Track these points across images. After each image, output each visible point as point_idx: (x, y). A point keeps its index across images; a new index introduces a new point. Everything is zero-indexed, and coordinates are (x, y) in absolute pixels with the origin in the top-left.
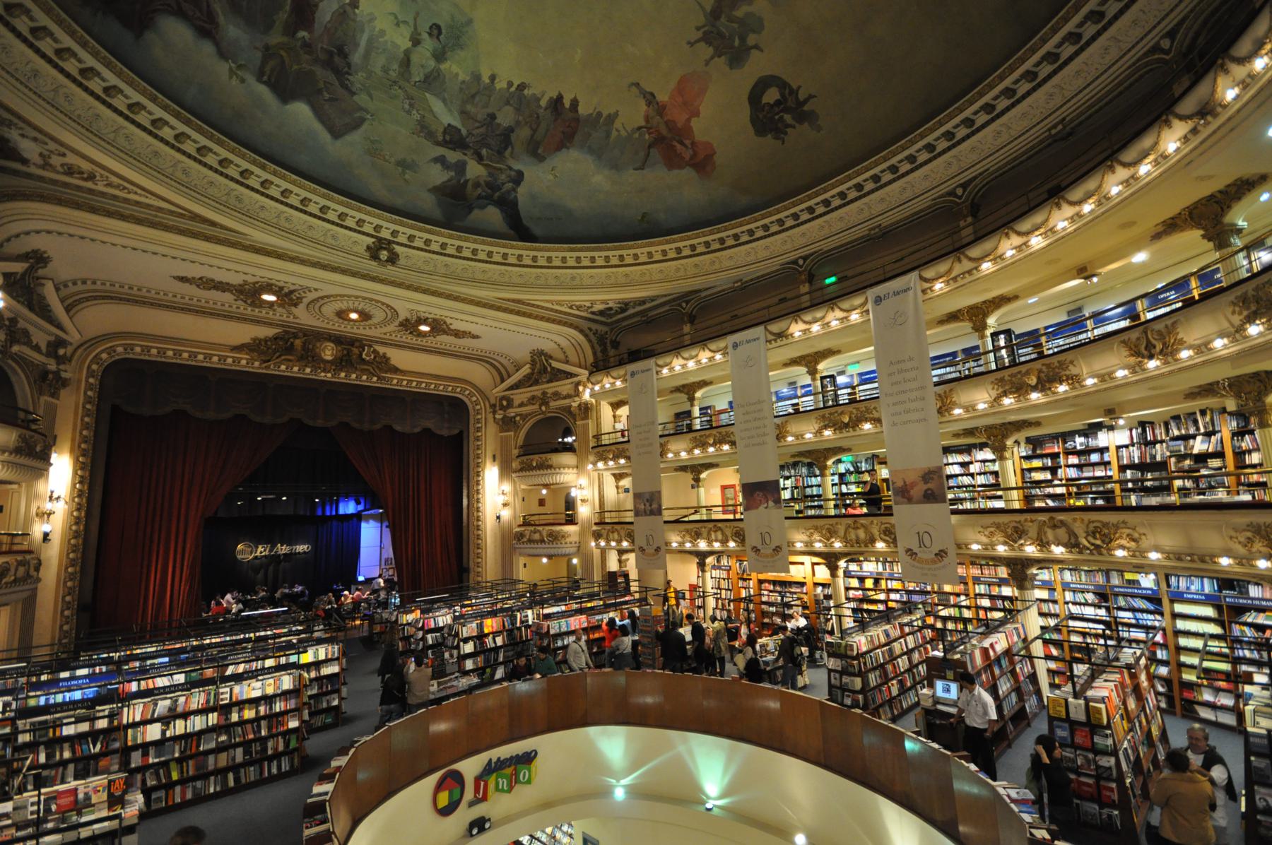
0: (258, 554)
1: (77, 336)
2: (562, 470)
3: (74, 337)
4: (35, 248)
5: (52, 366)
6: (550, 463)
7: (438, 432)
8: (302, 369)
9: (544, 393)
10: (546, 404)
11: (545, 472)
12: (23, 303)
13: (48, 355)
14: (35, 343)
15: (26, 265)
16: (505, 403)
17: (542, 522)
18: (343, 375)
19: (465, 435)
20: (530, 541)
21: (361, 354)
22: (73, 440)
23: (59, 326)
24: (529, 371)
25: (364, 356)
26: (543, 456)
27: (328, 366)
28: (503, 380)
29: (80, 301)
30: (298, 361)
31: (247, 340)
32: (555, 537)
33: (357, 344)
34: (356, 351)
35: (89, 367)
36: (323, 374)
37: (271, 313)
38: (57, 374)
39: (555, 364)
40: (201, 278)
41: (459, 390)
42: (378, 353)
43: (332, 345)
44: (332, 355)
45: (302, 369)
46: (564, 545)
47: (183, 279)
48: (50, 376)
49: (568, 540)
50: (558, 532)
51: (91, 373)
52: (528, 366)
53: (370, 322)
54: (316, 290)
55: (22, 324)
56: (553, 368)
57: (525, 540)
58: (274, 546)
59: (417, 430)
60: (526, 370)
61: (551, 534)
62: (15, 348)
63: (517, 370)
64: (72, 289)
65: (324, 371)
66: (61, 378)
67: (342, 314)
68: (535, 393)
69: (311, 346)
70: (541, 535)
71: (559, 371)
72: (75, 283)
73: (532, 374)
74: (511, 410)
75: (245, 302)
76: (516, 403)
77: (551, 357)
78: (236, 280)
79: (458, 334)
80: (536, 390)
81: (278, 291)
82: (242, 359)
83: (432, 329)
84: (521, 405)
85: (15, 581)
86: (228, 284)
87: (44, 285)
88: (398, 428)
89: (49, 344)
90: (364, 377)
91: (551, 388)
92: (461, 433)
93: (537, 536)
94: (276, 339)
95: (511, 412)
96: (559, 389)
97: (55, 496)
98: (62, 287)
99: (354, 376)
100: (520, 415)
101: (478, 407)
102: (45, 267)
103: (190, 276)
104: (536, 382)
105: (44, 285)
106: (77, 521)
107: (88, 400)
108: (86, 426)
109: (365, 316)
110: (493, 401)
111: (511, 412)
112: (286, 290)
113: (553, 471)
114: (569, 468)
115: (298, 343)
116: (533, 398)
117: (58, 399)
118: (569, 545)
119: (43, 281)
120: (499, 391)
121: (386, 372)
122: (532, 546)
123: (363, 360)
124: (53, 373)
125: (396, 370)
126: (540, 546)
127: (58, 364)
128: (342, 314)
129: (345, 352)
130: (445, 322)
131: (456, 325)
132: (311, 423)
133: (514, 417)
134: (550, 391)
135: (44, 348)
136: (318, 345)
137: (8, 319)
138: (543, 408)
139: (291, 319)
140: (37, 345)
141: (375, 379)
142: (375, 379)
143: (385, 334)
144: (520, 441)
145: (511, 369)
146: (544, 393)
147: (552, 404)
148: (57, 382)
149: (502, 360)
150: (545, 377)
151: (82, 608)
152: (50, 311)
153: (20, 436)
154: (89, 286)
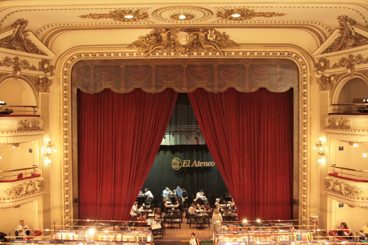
0: (184, 166)
1: (53, 55)
2: (357, 132)
3: (51, 56)
4: (18, 19)
5: (41, 75)
6: (348, 124)
7: (272, 90)
8: (169, 53)
9: (351, 56)
10: (351, 66)
11: (344, 132)
12: (19, 49)
13: (40, 70)
14: (31, 66)
15: (17, 29)
16: (322, 64)
17: (344, 176)
18: (195, 54)
19: (295, 91)
20: (333, 190)
21: (206, 36)
22: (60, 112)
23: (43, 53)
24: (339, 35)
25: (209, 38)
26: (344, 116)
27: (183, 49)
28: (322, 42)
29: (52, 35)
30: (165, 48)
31: (135, 39)
32: (350, 191)
33: (201, 30)
34: (202, 35)
35: (63, 70)
36: (182, 56)
37: (138, 23)
38: (46, 80)
39: (357, 30)
40: (90, 15)
41: (286, 54)
42: (219, 33)
43: (186, 33)
44: (187, 40)
45: (169, 53)
46: (356, 200)
47: (84, 17)
48: (41, 81)
49: (360, 195)
50: (352, 188)
51: (65, 73)
52: (337, 31)
53: (195, 18)
54: (148, 8)
55: (21, 59)
56: (356, 33)
57: (330, 188)
58: (192, 161)
59: (254, 90)
60: (336, 34)
61: (347, 189)
62: (18, 73)
63: (331, 34)
64: (45, 31)
65: (182, 53)
66: (48, 80)
67: (175, 17)
68: (344, 56)
69: (172, 37)
70: (341, 188)
71: (360, 35)
72: (45, 28)
73: (342, 37)
74: (327, 71)
75: (120, 20)
76: (331, 64)
77: (354, 23)
78: (107, 12)
79: (263, 15)
80: (345, 53)
81: (130, 12)
82: (133, 52)
83: (242, 15)
84: (335, 66)
85: (27, 193)
86: (104, 14)
87: (28, 35)
88: (239, 89)
89: (39, 62)
90: (210, 54)
91: (356, 51)
92: (292, 89)
93: (337, 188)
94: (151, 35)
95: (328, 73)
96: (361, 53)
97: (52, 144)
98: (40, 32)
99: (203, 54)
100: (333, 75)
101: (304, 67)
102: (27, 25)
103: (85, 15)
104: (344, 46)
105: (28, 35)
106: (66, 155)
107: (65, 89)
108: (65, 103)
109: (189, 17)
110: (317, 61)
111: (328, 73)
112: (133, 12)
113: (350, 132)
114: (363, 131)
115: (164, 35)
116: (343, 60)
117: (49, 92)
118: (360, 200)
119: (28, 33)
120: (317, 54)
121: (225, 47)
122: (334, 194)
123: (208, 40)
124: (43, 78)
125: (234, 45)
126: (339, 196)
127: (45, 73)
128: (175, 17)
129: (195, 37)
130: (248, 10)
131: (257, 11)
132: (178, 90)
133: (329, 78)
134: (355, 54)
135: (37, 67)
136: (177, 34)
137: (14, 59)
138: (349, 71)
139: (150, 23)
140: (33, 66)
141: (218, 54)
142: (218, 54)
143: (213, 22)
144: (335, 100)
145: (327, 33)
146: (351, 56)
147: (357, 67)
148: (47, 82)
149: (320, 27)
150: (351, 42)
151: (75, 201)
152: (36, 46)
153: (19, 122)
154: (51, 28)
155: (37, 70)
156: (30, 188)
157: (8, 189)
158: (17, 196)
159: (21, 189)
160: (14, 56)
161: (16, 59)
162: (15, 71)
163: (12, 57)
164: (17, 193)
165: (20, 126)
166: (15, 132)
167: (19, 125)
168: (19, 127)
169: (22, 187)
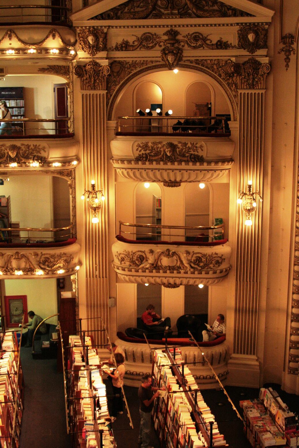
14: (214, 42)
155: (233, 47)
156: (165, 261)
157: (119, 253)
158: (133, 266)
159: (142, 259)
160: (166, 29)
161: (173, 34)
162: (164, 56)
163: (160, 31)
164: (132, 262)
165: (143, 152)
166: (129, 162)
167: (140, 151)
168: (141, 153)
169: (144, 256)
